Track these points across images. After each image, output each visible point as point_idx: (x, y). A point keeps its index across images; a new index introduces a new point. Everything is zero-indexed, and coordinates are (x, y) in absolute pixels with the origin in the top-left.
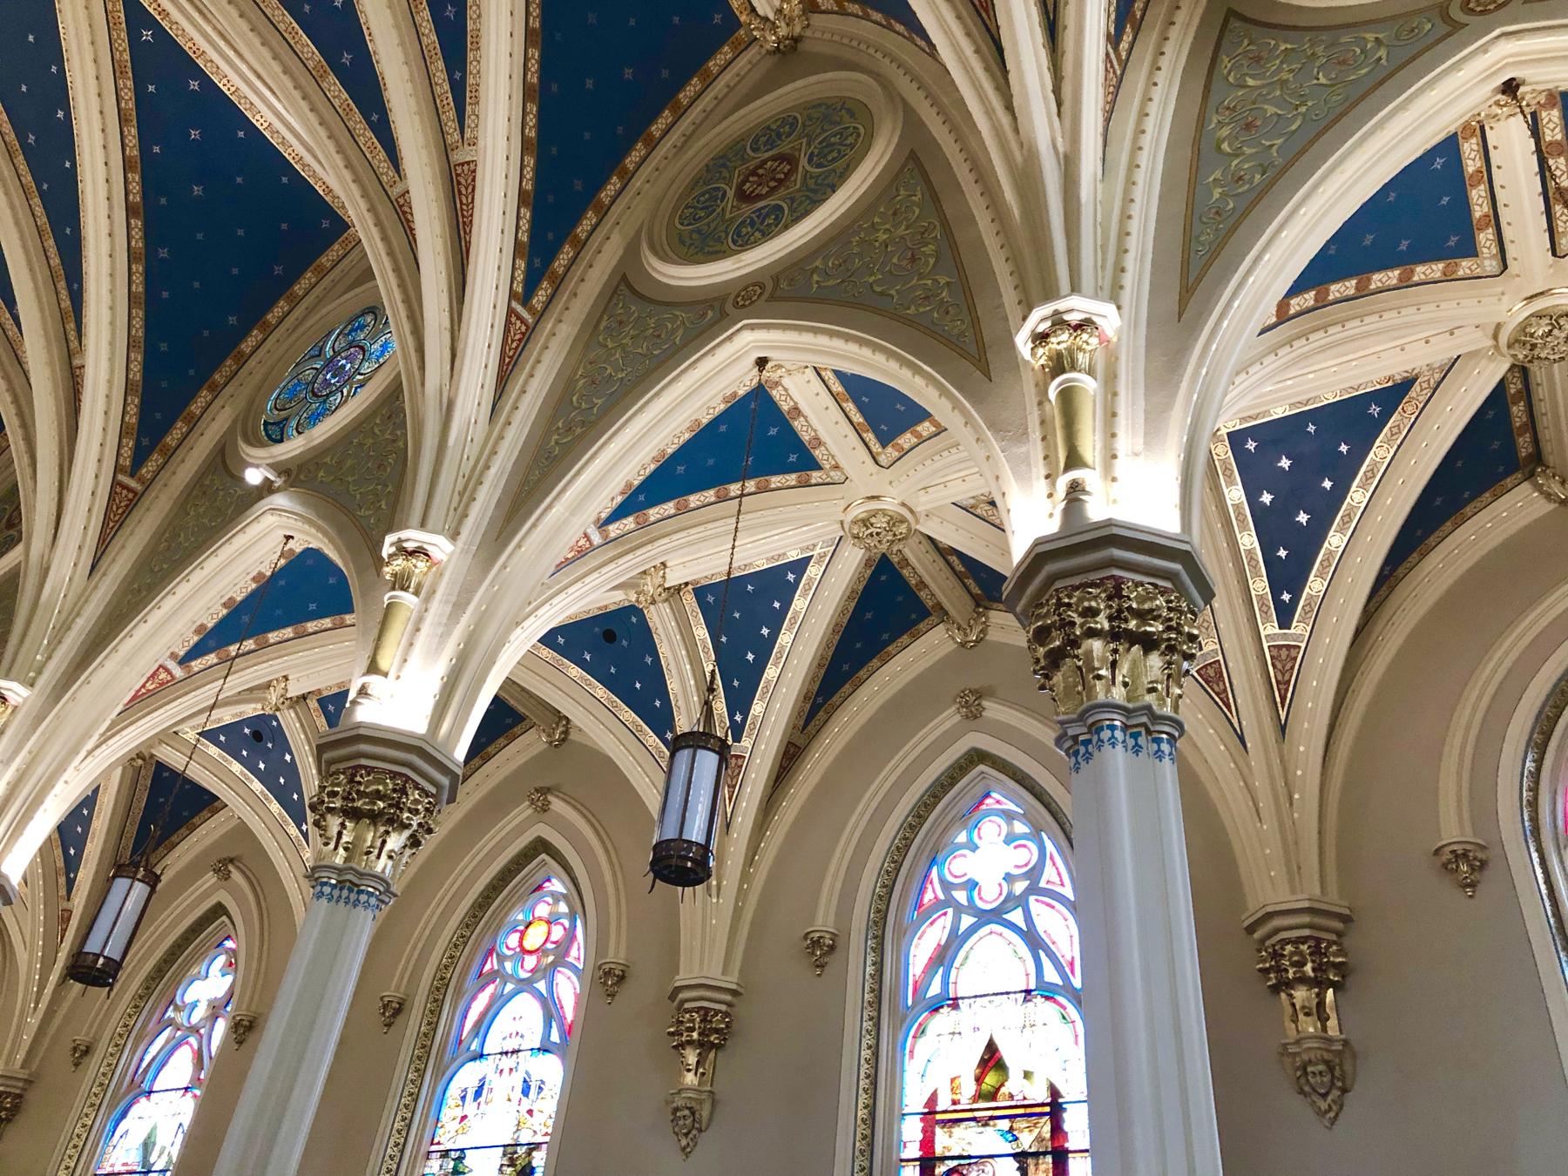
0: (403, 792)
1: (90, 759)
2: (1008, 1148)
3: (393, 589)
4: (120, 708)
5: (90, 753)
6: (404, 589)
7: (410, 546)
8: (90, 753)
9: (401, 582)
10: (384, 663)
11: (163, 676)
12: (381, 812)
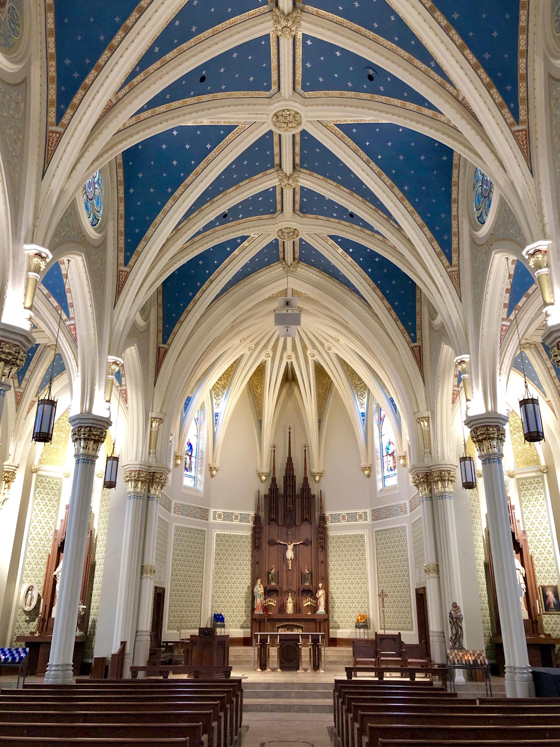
0: (488, 430)
1: (502, 371)
2: (526, 529)
3: (537, 270)
4: (499, 345)
5: (500, 369)
6: (541, 268)
7: (531, 252)
8: (500, 369)
9: (538, 266)
10: (548, 300)
11: (504, 328)
12: (486, 437)
